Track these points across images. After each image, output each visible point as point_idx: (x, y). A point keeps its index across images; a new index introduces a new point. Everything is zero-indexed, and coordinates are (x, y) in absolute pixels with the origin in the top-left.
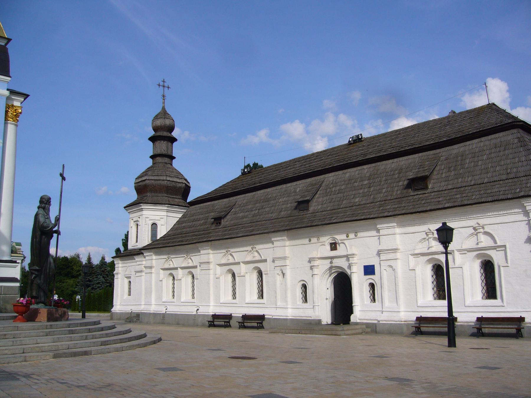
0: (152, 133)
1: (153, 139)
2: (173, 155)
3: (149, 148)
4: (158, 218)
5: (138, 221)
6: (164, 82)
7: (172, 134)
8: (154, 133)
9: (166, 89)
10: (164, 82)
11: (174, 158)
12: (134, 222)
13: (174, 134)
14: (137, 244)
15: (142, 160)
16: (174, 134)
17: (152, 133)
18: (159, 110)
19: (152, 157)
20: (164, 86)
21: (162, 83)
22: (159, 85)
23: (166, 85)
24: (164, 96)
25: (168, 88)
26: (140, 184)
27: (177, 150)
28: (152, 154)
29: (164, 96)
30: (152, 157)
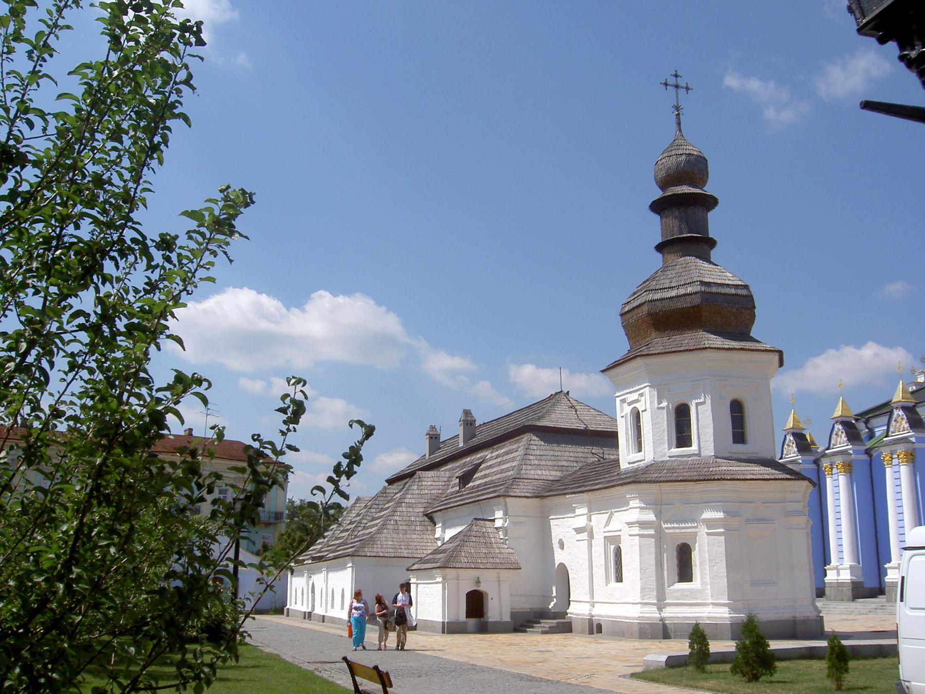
1: (658, 207)
2: (711, 235)
6: (676, 76)
9: (682, 92)
10: (676, 76)
11: (712, 243)
12: (629, 404)
20: (677, 87)
21: (672, 81)
22: (666, 84)
23: (681, 82)
24: (677, 108)
25: (687, 89)
27: (716, 223)
29: (677, 108)
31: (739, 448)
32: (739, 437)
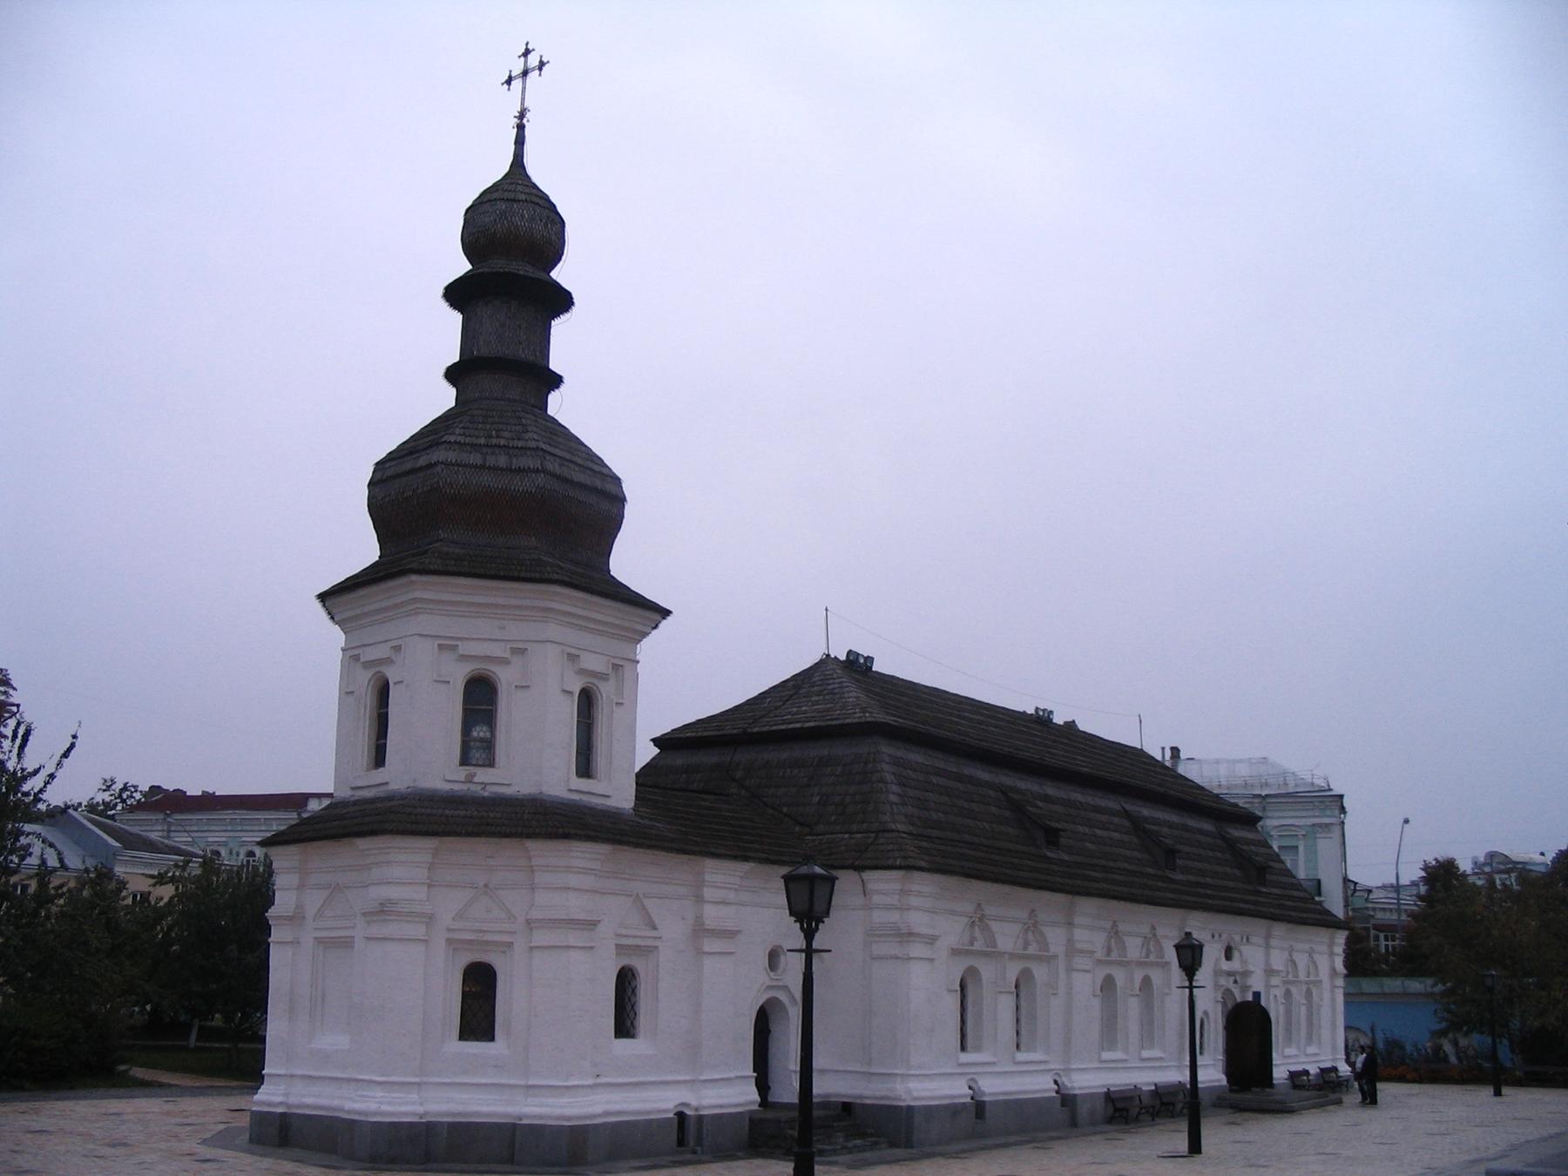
0: (461, 266)
3: (445, 334)
4: (497, 650)
5: (388, 661)
7: (554, 274)
8: (465, 266)
11: (556, 381)
12: (368, 665)
13: (561, 274)
14: (379, 776)
16: (561, 274)
17: (461, 266)
18: (501, 168)
19: (452, 374)
27: (566, 343)
28: (455, 357)
30: (452, 374)
32: (585, 767)
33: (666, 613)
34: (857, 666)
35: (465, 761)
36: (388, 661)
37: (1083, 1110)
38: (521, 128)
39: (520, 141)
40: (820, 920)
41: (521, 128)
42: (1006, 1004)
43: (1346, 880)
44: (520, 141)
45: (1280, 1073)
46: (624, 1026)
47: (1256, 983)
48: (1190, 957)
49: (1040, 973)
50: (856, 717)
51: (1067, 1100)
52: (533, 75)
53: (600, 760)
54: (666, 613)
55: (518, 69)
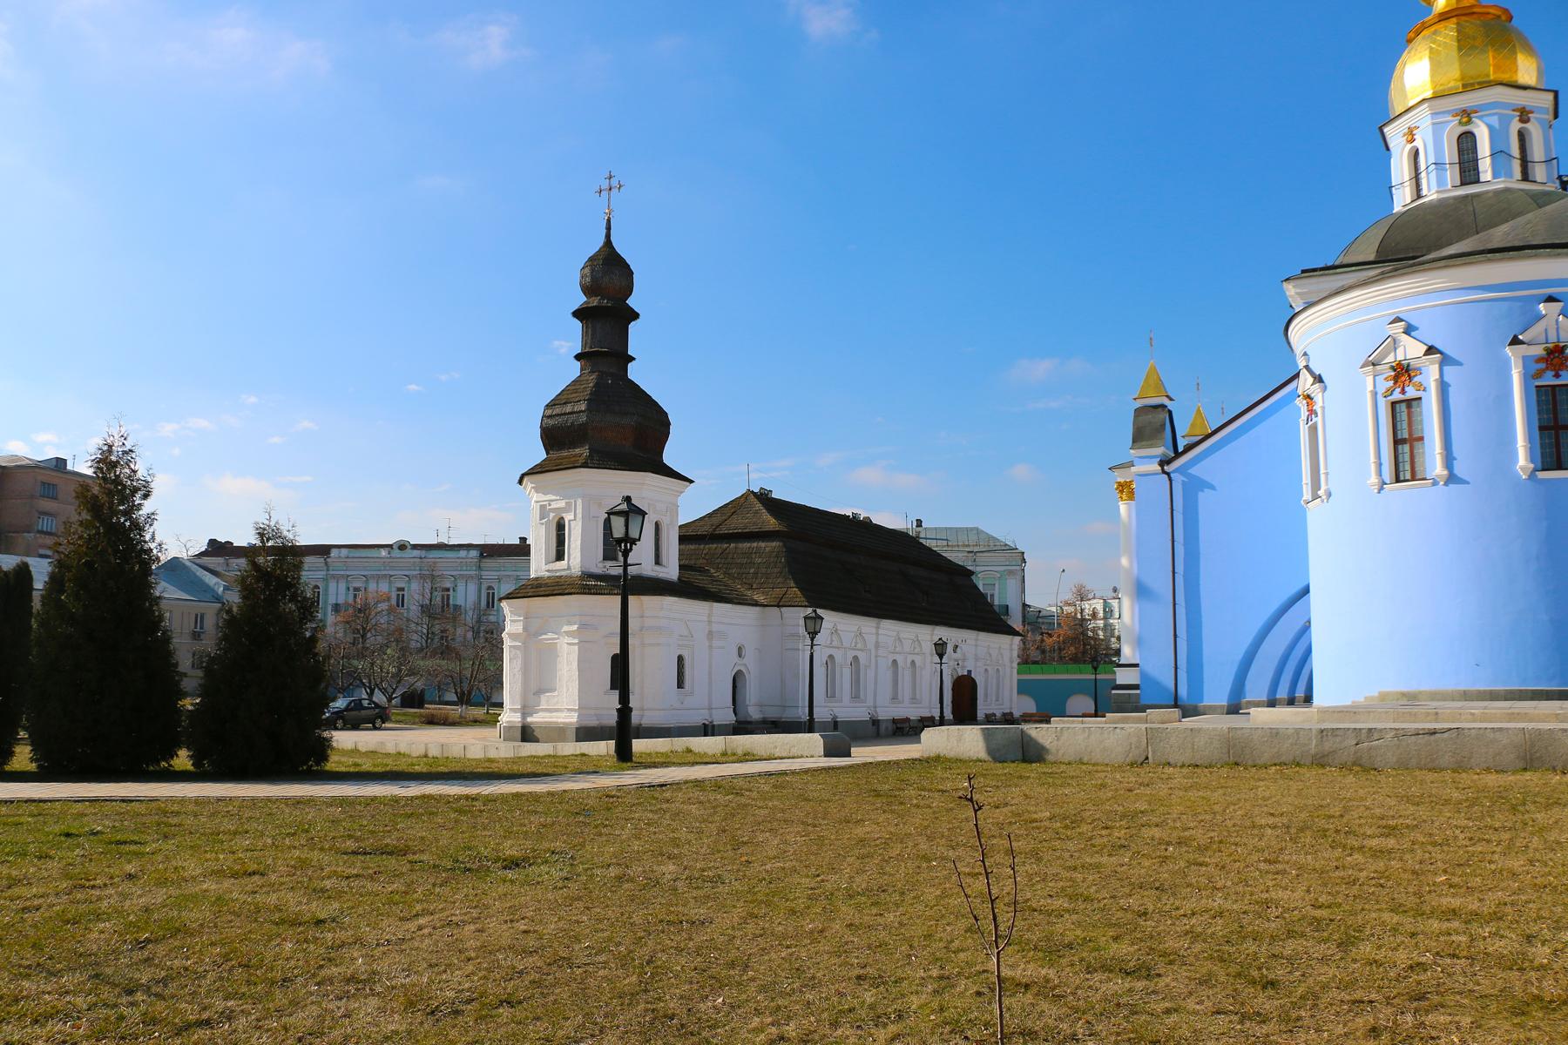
0: (580, 299)
14: (562, 564)
15: (557, 360)
17: (580, 299)
18: (599, 242)
19: (578, 357)
26: (551, 422)
27: (638, 338)
30: (578, 357)
31: (657, 568)
33: (691, 482)
34: (764, 497)
35: (605, 558)
36: (567, 509)
37: (883, 727)
38: (609, 221)
39: (609, 228)
40: (816, 633)
41: (609, 221)
42: (847, 672)
43: (1025, 606)
44: (609, 228)
45: (980, 715)
46: (680, 685)
47: (970, 665)
48: (940, 649)
49: (862, 656)
50: (771, 528)
51: (875, 722)
52: (614, 191)
53: (664, 560)
54: (691, 482)
55: (605, 185)
